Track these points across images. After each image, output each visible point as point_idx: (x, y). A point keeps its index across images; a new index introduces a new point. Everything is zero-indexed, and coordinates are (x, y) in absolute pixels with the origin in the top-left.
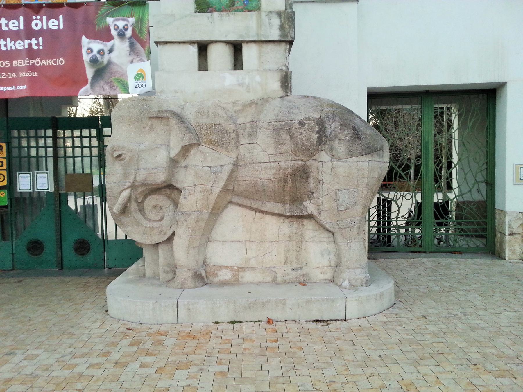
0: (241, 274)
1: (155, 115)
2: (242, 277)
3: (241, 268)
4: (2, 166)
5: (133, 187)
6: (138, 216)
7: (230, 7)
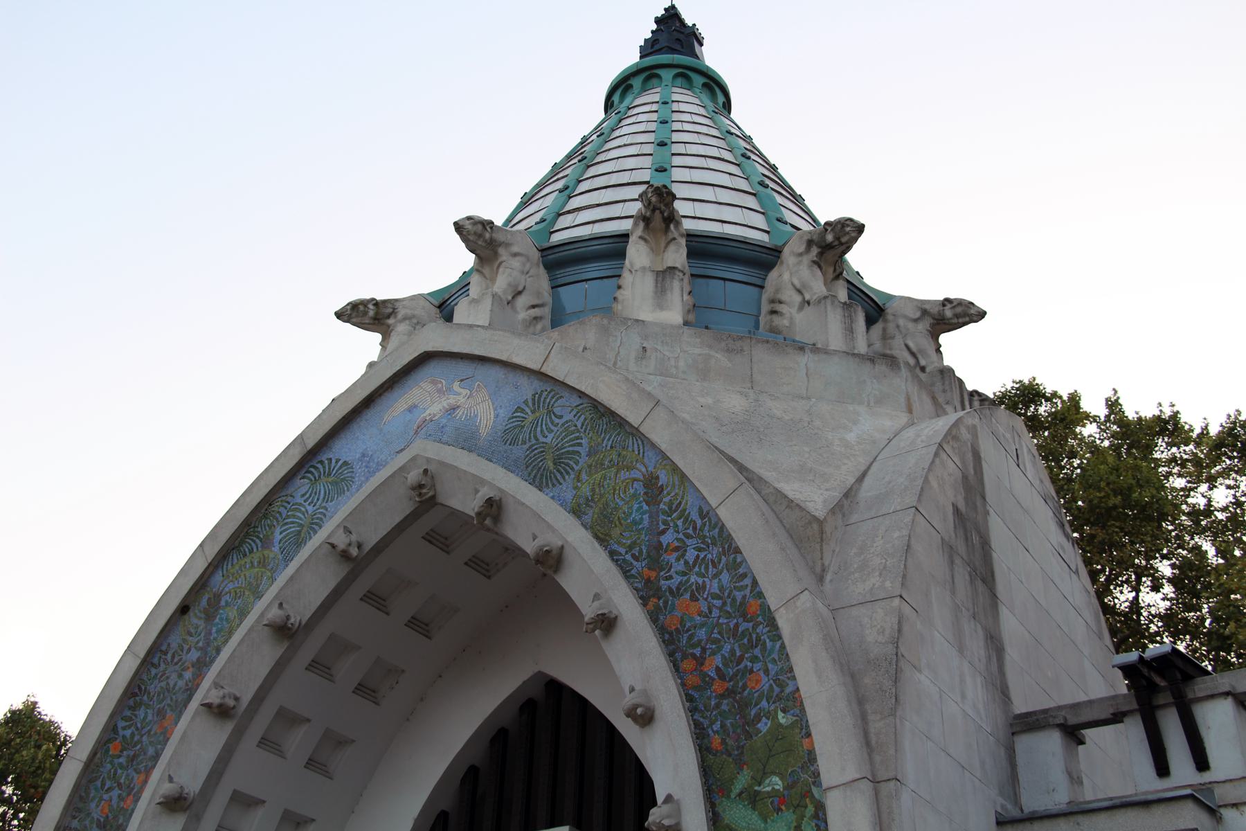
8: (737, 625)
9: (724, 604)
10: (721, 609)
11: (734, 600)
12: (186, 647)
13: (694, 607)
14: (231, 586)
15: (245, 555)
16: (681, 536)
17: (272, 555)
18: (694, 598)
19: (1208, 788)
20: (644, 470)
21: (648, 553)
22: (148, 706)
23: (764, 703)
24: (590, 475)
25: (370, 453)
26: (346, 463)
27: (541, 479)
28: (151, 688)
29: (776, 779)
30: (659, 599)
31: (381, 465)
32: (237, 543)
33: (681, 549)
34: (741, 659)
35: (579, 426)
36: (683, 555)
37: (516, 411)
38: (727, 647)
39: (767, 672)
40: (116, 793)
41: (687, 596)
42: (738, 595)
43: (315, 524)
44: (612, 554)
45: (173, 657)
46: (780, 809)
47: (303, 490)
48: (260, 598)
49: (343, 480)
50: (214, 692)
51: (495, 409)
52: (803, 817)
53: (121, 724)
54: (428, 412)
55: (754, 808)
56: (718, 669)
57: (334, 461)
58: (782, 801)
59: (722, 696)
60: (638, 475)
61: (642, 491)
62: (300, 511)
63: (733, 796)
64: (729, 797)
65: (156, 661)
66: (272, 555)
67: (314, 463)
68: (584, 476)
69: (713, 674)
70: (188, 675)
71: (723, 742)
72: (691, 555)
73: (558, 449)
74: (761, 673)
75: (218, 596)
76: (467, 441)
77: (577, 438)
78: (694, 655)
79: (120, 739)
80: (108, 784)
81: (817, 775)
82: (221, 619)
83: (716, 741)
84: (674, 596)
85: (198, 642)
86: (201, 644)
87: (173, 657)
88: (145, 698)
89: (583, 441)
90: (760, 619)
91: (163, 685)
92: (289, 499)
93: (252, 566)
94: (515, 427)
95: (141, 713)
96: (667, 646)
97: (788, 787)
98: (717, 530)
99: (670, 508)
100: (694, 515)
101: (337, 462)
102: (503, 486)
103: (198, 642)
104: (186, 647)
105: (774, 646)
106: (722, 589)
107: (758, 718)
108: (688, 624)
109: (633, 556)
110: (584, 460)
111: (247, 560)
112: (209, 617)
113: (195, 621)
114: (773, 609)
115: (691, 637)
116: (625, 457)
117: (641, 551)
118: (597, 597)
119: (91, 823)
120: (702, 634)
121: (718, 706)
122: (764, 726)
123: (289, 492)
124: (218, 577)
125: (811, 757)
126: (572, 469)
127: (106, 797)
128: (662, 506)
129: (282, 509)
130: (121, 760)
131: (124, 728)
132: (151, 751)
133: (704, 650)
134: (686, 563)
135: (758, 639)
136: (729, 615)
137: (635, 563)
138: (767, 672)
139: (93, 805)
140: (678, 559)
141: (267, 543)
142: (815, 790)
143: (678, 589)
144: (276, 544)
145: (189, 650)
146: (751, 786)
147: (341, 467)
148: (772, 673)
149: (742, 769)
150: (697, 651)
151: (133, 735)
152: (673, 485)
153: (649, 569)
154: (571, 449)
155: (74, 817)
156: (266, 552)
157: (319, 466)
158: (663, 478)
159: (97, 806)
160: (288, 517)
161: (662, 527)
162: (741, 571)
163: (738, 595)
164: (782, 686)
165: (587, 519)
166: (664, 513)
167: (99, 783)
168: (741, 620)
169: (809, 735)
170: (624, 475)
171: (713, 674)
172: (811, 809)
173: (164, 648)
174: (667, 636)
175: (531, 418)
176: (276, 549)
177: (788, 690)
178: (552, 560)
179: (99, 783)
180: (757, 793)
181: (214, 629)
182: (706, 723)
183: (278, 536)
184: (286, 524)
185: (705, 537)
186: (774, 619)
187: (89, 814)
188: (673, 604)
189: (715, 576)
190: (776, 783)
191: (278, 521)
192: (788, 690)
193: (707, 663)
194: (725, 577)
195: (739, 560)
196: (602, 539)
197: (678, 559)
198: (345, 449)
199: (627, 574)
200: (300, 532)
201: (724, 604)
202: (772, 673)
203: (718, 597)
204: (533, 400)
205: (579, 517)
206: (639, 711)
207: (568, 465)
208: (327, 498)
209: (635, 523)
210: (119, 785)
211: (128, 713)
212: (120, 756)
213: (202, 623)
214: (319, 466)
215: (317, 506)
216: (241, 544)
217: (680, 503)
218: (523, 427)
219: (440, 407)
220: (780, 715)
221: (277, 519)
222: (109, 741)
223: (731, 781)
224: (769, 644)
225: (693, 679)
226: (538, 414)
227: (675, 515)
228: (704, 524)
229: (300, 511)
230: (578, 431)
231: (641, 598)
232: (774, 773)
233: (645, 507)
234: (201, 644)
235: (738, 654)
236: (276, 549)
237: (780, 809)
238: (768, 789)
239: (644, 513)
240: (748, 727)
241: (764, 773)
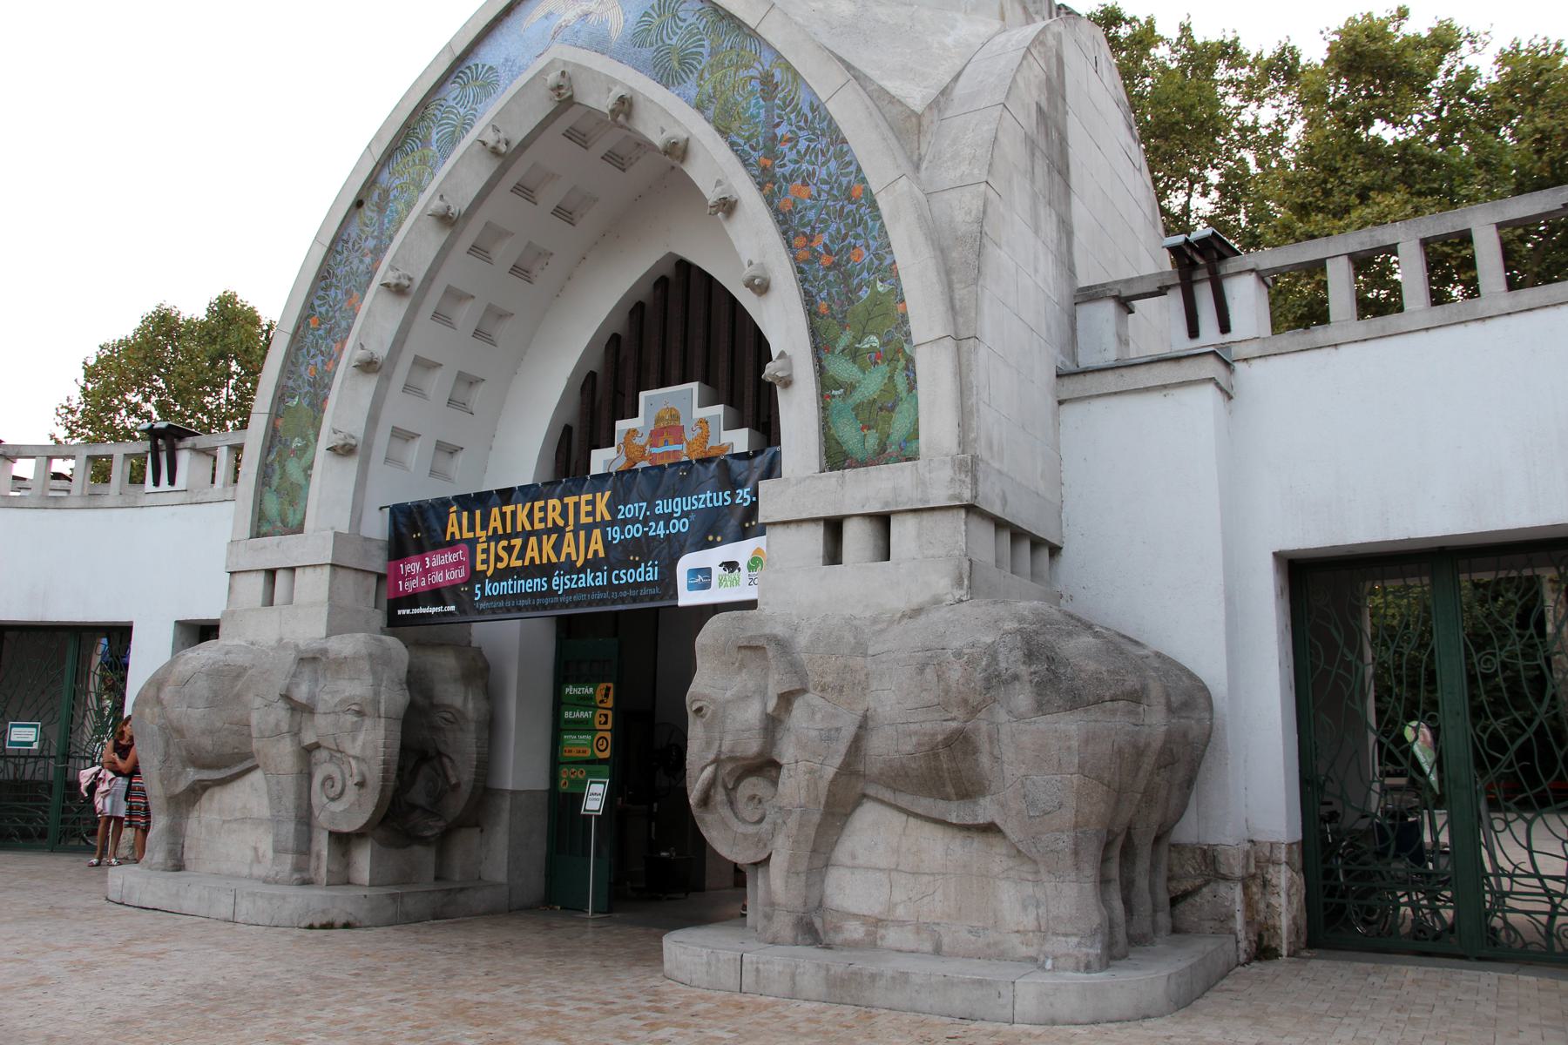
0: (881, 932)
1: (745, 644)
2: (882, 938)
3: (881, 920)
4: (606, 723)
5: (717, 761)
6: (725, 812)
7: (879, 454)
8: (842, 207)
9: (832, 188)
10: (828, 193)
11: (840, 185)
12: (364, 237)
13: (805, 191)
14: (397, 182)
15: (407, 154)
16: (794, 128)
17: (431, 154)
18: (805, 184)
19: (1227, 346)
20: (760, 68)
21: (764, 143)
22: (337, 287)
23: (865, 274)
24: (712, 74)
25: (513, 58)
26: (491, 68)
27: (667, 78)
28: (338, 272)
29: (873, 338)
30: (774, 184)
31: (522, 69)
32: (399, 144)
33: (794, 140)
34: (846, 235)
35: (701, 27)
36: (796, 146)
37: (644, 16)
39: (868, 247)
40: (319, 359)
41: (799, 182)
42: (844, 181)
43: (466, 125)
44: (732, 145)
45: (354, 245)
46: (876, 363)
47: (454, 94)
48: (423, 191)
49: (489, 84)
50: (390, 274)
51: (625, 14)
52: (895, 369)
53: (317, 303)
54: (563, 18)
55: (854, 362)
56: (825, 245)
57: (480, 66)
58: (878, 357)
59: (829, 268)
60: (754, 73)
61: (758, 87)
62: (453, 113)
63: (837, 352)
64: (834, 352)
65: (339, 249)
66: (431, 154)
67: (462, 69)
68: (707, 75)
69: (821, 249)
70: (368, 260)
71: (829, 307)
72: (802, 145)
73: (683, 51)
74: (863, 248)
75: (387, 191)
76: (600, 45)
77: (700, 40)
78: (804, 234)
79: (317, 315)
80: (312, 352)
81: (908, 334)
82: (391, 211)
83: (823, 307)
84: (787, 182)
85: (373, 232)
86: (376, 234)
87: (354, 245)
88: (334, 280)
89: (705, 43)
90: (863, 201)
91: (348, 268)
92: (442, 102)
93: (415, 164)
94: (643, 31)
95: (332, 293)
96: (781, 225)
97: (883, 345)
98: (826, 123)
99: (784, 103)
100: (806, 110)
101: (483, 67)
102: (633, 85)
103: (373, 232)
104: (364, 237)
105: (874, 226)
106: (829, 175)
107: (860, 287)
108: (800, 207)
109: (751, 147)
110: (706, 60)
111: (410, 158)
112: (381, 209)
113: (370, 214)
114: (874, 192)
115: (802, 218)
116: (743, 57)
117: (758, 143)
118: (719, 183)
119: (303, 382)
120: (812, 215)
121: (825, 277)
122: (865, 294)
123: (442, 95)
124: (385, 175)
125: (904, 319)
126: (696, 68)
127: (311, 361)
128: (777, 101)
129: (436, 112)
130: (320, 332)
131: (319, 306)
132: (344, 324)
133: (813, 228)
134: (798, 152)
135: (861, 219)
136: (836, 199)
137: (752, 153)
138: (868, 247)
139: (303, 368)
140: (791, 149)
141: (425, 142)
142: (906, 347)
143: (791, 175)
144: (434, 143)
145: (367, 238)
146: (852, 344)
147: (487, 72)
148: (872, 248)
149: (845, 329)
150: (808, 230)
151: (327, 311)
152: (787, 81)
153: (766, 158)
154: (694, 50)
155: (289, 378)
156: (425, 151)
157: (467, 71)
159: (306, 369)
160: (442, 119)
161: (777, 120)
162: (847, 159)
163: (844, 181)
164: (881, 259)
165: (710, 113)
166: (779, 107)
167: (305, 351)
168: (846, 202)
169: (903, 301)
170: (742, 73)
171: (821, 249)
172: (902, 362)
173: (345, 238)
174: (781, 217)
175: (657, 21)
176: (434, 148)
177: (886, 263)
178: (678, 151)
179: (305, 351)
180: (857, 350)
181: (386, 220)
182: (814, 291)
183: (435, 137)
184: (442, 125)
185: (816, 128)
186: (875, 201)
187: (301, 376)
188: (786, 189)
189: (824, 164)
190: (873, 341)
191: (434, 123)
192: (886, 263)
193: (816, 240)
194: (833, 165)
195: (845, 149)
196: (723, 132)
197: (791, 149)
198: (490, 55)
199: (745, 163)
200: (454, 132)
201: (832, 188)
202: (872, 248)
203: (826, 182)
204: (659, 4)
205: (702, 112)
206: (756, 282)
207: (692, 65)
208: (475, 102)
209: (753, 117)
210: (321, 352)
211: (321, 293)
212: (318, 330)
213: (374, 215)
214: (467, 71)
215: (468, 108)
216: (402, 145)
217: (793, 99)
218: (650, 30)
219: (574, 13)
220: (879, 284)
221: (433, 121)
222: (309, 317)
223: (836, 340)
224: (870, 223)
225: (803, 254)
226: (663, 18)
227: (789, 109)
228: (814, 117)
229: (453, 113)
230: (701, 34)
231: (758, 183)
232: (872, 333)
233: (762, 102)
234: (376, 234)
235: (843, 232)
236: (434, 148)
237: (876, 363)
238: (867, 346)
239: (761, 107)
240: (850, 296)
241: (864, 333)
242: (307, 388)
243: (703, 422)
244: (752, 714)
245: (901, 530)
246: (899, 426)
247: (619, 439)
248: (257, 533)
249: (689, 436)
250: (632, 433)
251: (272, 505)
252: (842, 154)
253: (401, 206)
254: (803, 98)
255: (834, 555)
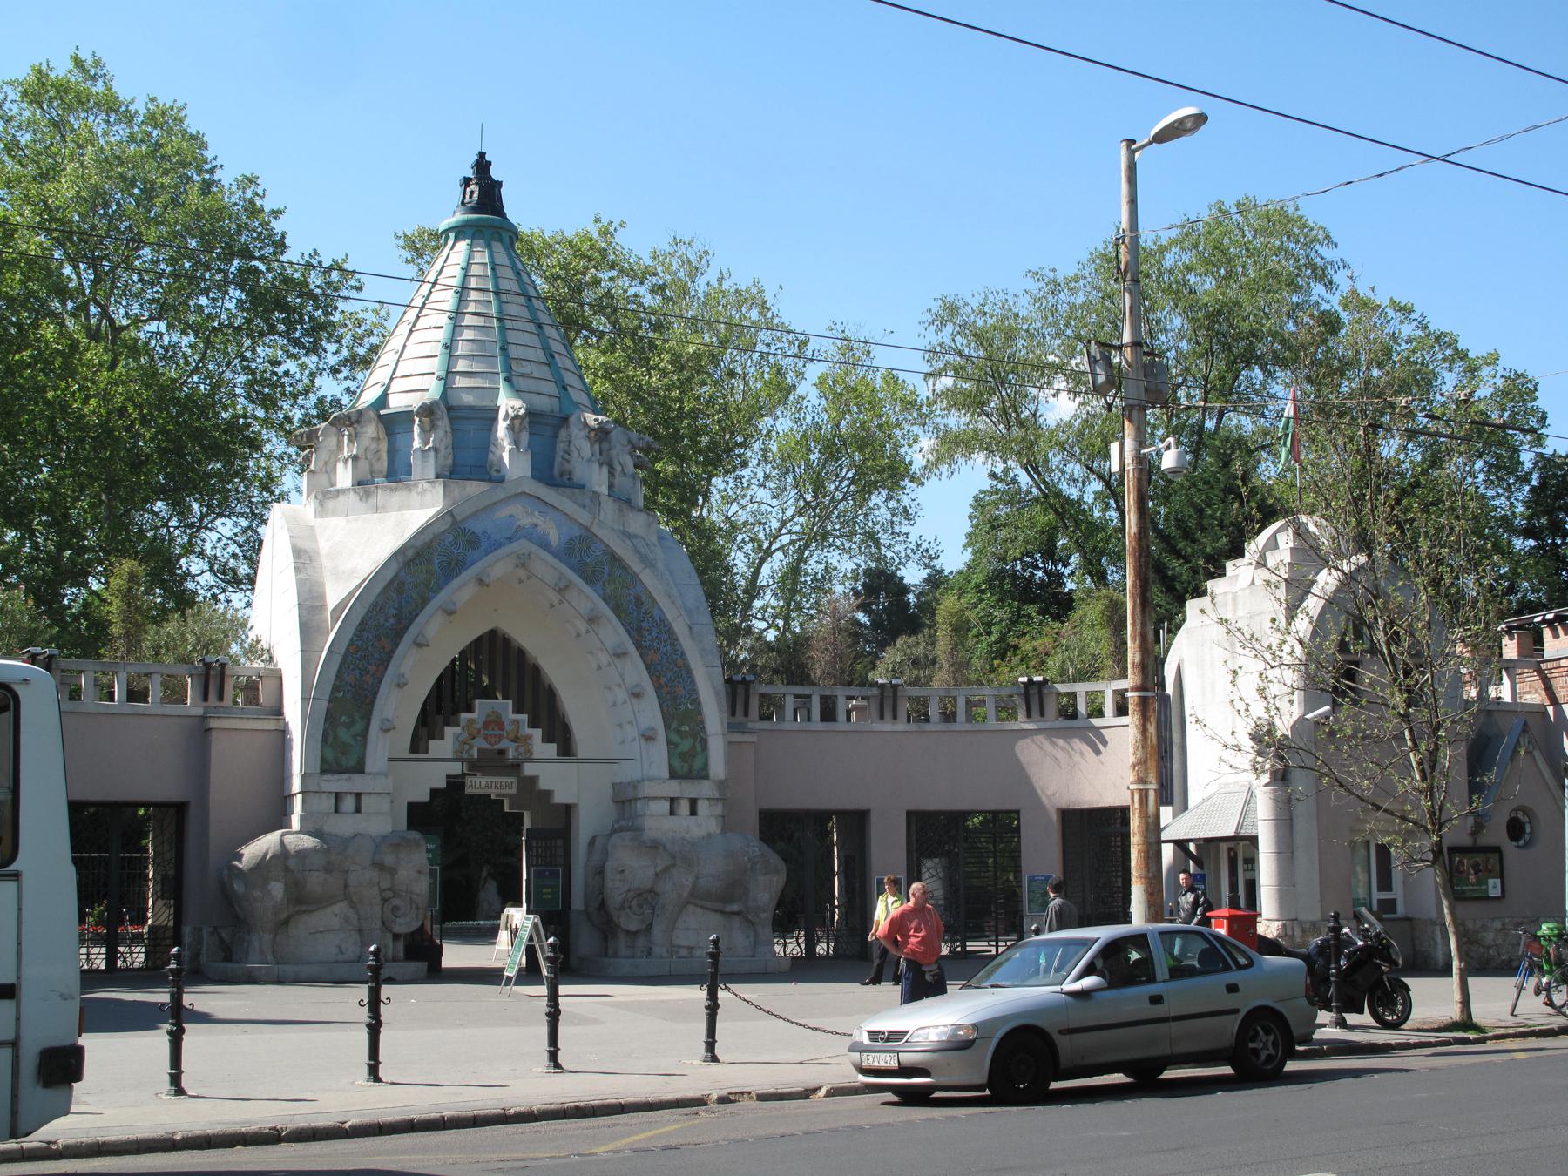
38: (669, 675)
59: (667, 693)
72: (654, 634)
95: (365, 634)
110: (606, 576)
120: (659, 668)
122: (682, 707)
125: (702, 722)
158: (644, 599)
213: (394, 595)
242: (349, 688)
243: (516, 722)
244: (651, 872)
245: (702, 807)
246: (698, 763)
247: (463, 723)
248: (323, 771)
249: (508, 727)
250: (471, 721)
251: (330, 755)
252: (673, 645)
253: (415, 595)
254: (656, 613)
255: (672, 813)
